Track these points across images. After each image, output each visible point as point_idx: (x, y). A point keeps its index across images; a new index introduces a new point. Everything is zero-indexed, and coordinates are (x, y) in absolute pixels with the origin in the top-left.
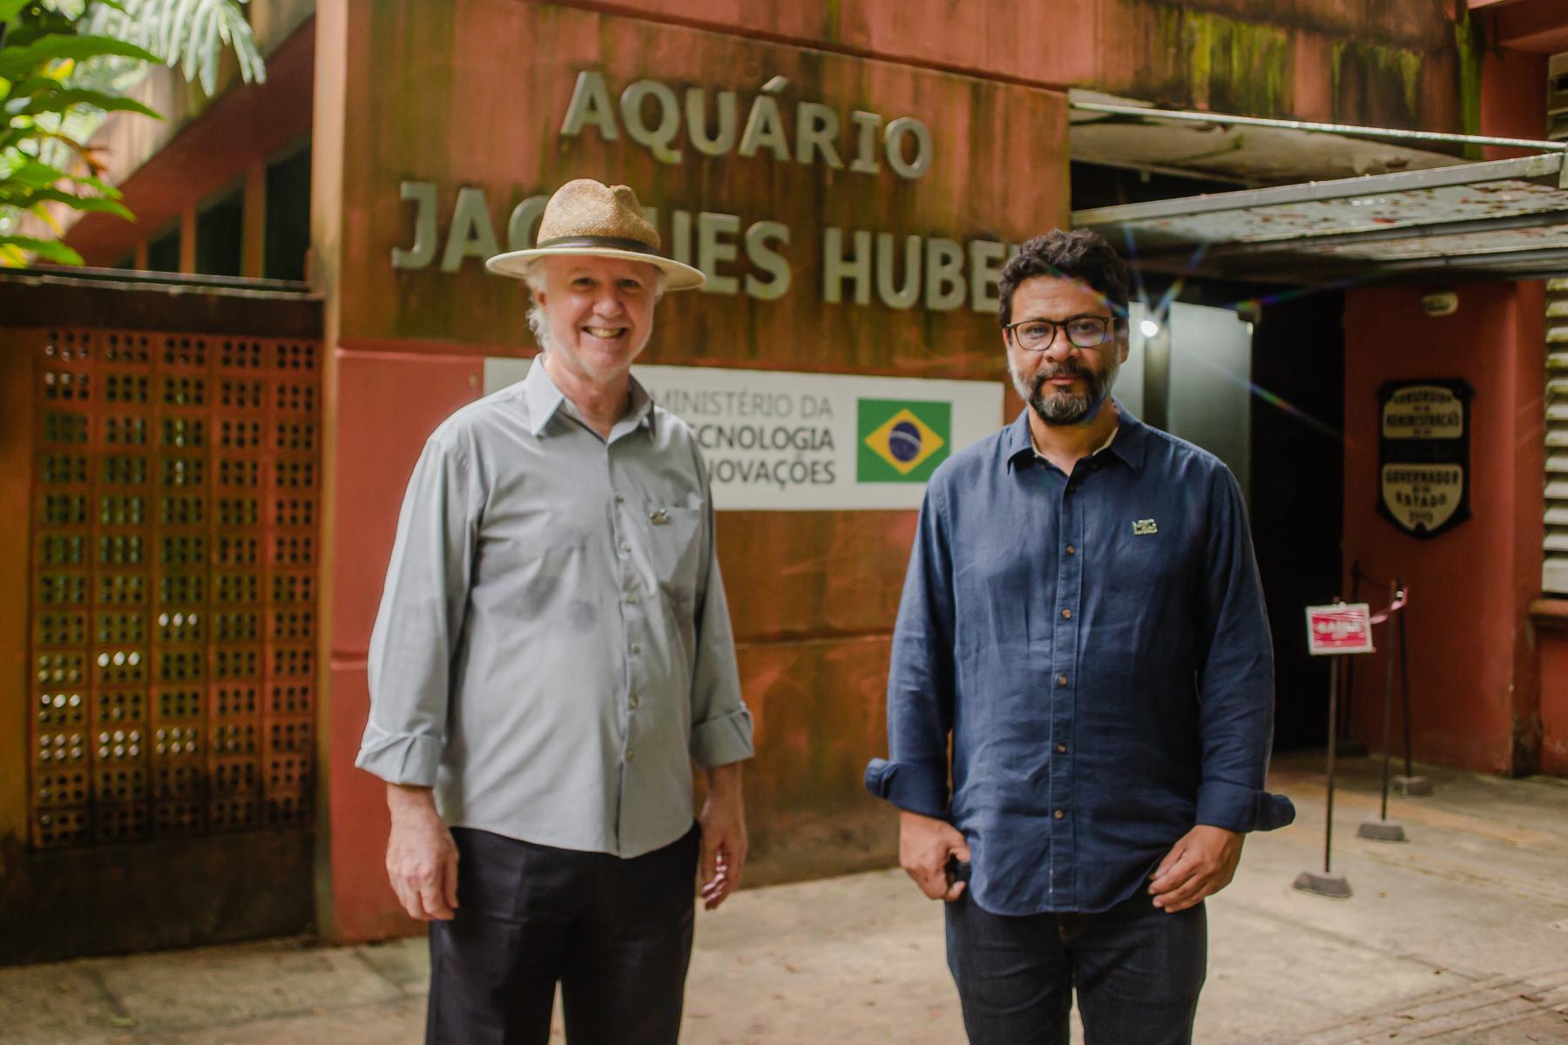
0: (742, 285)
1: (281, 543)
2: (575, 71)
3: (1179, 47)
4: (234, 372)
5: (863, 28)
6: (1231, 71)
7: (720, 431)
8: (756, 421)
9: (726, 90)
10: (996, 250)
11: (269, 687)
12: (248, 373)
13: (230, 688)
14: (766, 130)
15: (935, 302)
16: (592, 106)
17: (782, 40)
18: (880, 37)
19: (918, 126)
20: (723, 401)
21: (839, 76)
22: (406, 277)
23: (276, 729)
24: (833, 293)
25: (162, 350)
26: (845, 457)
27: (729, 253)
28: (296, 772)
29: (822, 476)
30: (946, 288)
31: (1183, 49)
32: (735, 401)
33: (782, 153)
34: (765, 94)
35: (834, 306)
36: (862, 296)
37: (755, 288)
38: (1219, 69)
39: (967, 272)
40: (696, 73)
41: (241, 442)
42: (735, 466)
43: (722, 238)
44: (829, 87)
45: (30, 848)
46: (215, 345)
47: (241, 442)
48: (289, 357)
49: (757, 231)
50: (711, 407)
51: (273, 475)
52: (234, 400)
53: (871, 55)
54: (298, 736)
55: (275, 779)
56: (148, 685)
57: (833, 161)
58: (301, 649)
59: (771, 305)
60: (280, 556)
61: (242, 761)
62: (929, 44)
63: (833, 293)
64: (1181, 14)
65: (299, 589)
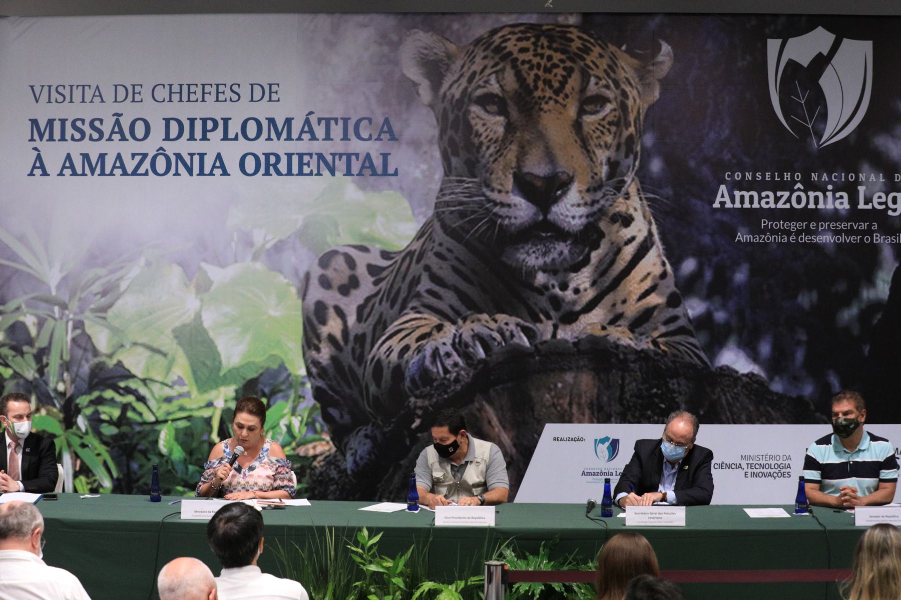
8: (769, 462)
20: (761, 457)
29: (787, 475)
32: (764, 457)
42: (763, 473)
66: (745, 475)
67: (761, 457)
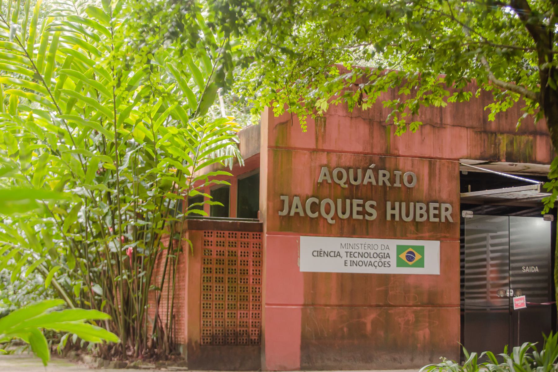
0: (364, 217)
1: (253, 279)
2: (321, 166)
3: (495, 144)
4: (243, 240)
5: (397, 149)
6: (513, 149)
7: (359, 253)
9: (359, 168)
10: (437, 205)
11: (251, 313)
12: (246, 240)
13: (242, 312)
14: (370, 178)
15: (418, 219)
16: (325, 175)
17: (375, 154)
18: (402, 151)
19: (412, 173)
20: (360, 246)
21: (391, 162)
22: (283, 217)
23: (252, 322)
24: (389, 218)
25: (228, 235)
26: (393, 260)
27: (360, 209)
28: (257, 332)
29: (387, 265)
30: (421, 216)
31: (497, 145)
32: (363, 246)
33: (374, 183)
34: (370, 168)
35: (389, 221)
36: (397, 218)
37: (367, 217)
38: (509, 150)
39: (428, 211)
40: (352, 164)
41: (244, 256)
43: (358, 205)
44: (387, 165)
45: (200, 345)
46: (239, 233)
47: (244, 256)
48: (255, 236)
49: (368, 203)
50: (356, 247)
51: (252, 263)
52: (243, 246)
53: (399, 156)
54: (257, 324)
55: (252, 334)
56: (225, 310)
57: (388, 184)
58: (258, 304)
59: (372, 221)
60: (253, 282)
61: (245, 329)
62: (417, 150)
63: (389, 218)
64: (496, 135)
65: (257, 290)
66: (345, 263)
67: (360, 246)
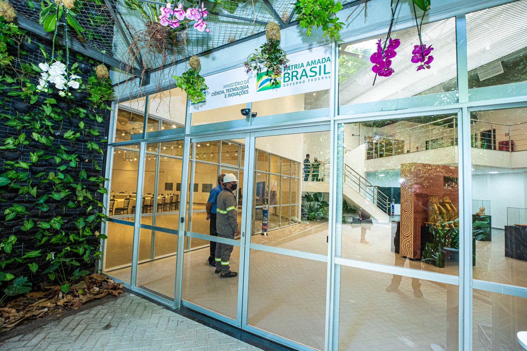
67: (233, 84)
